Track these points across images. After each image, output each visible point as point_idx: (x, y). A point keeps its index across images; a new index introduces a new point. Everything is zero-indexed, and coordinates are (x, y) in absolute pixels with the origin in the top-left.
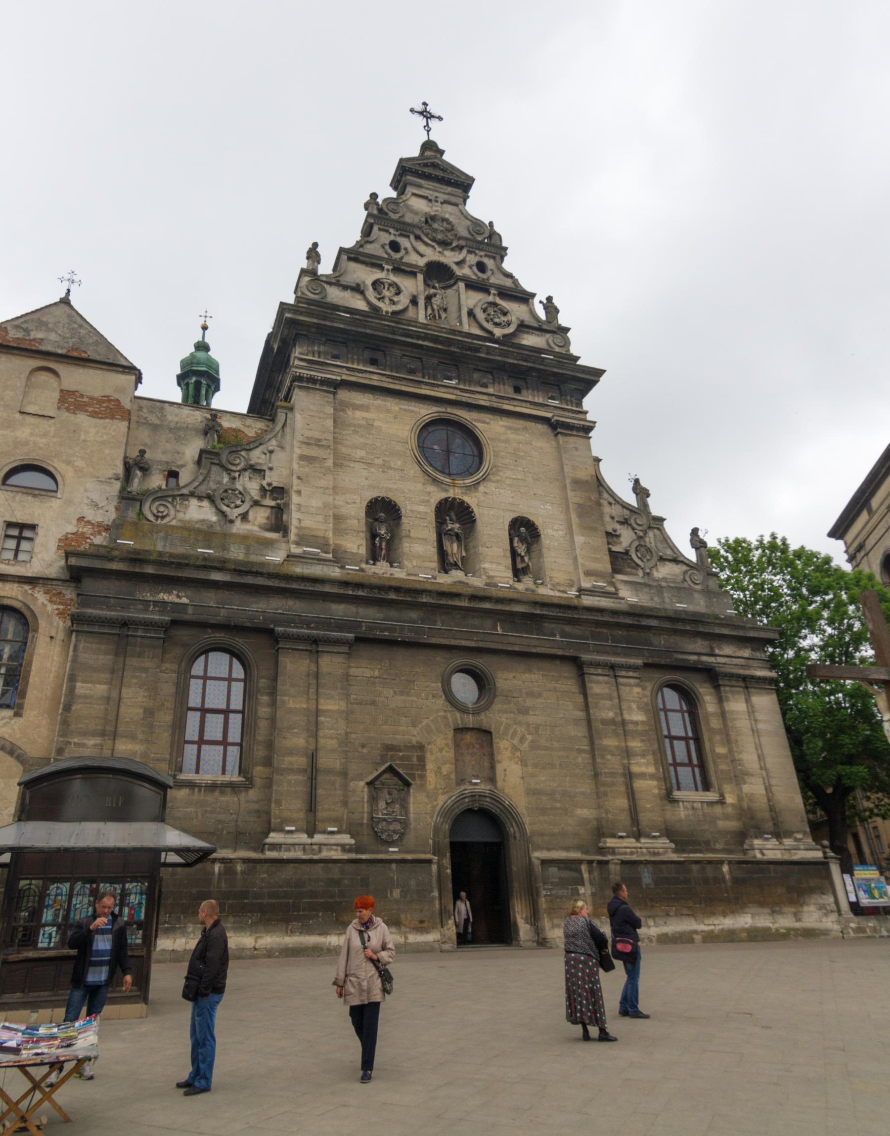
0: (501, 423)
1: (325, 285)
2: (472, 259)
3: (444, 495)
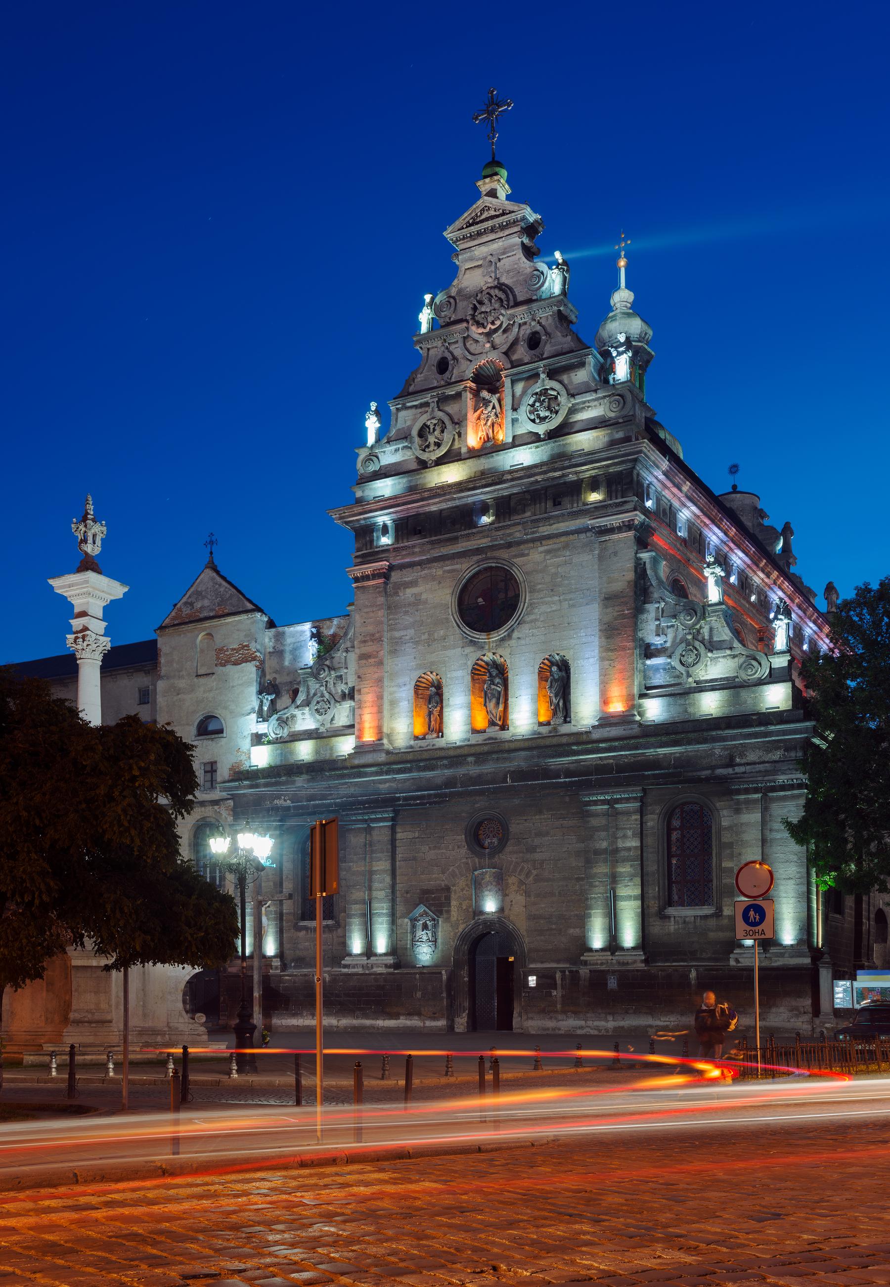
0: (541, 549)
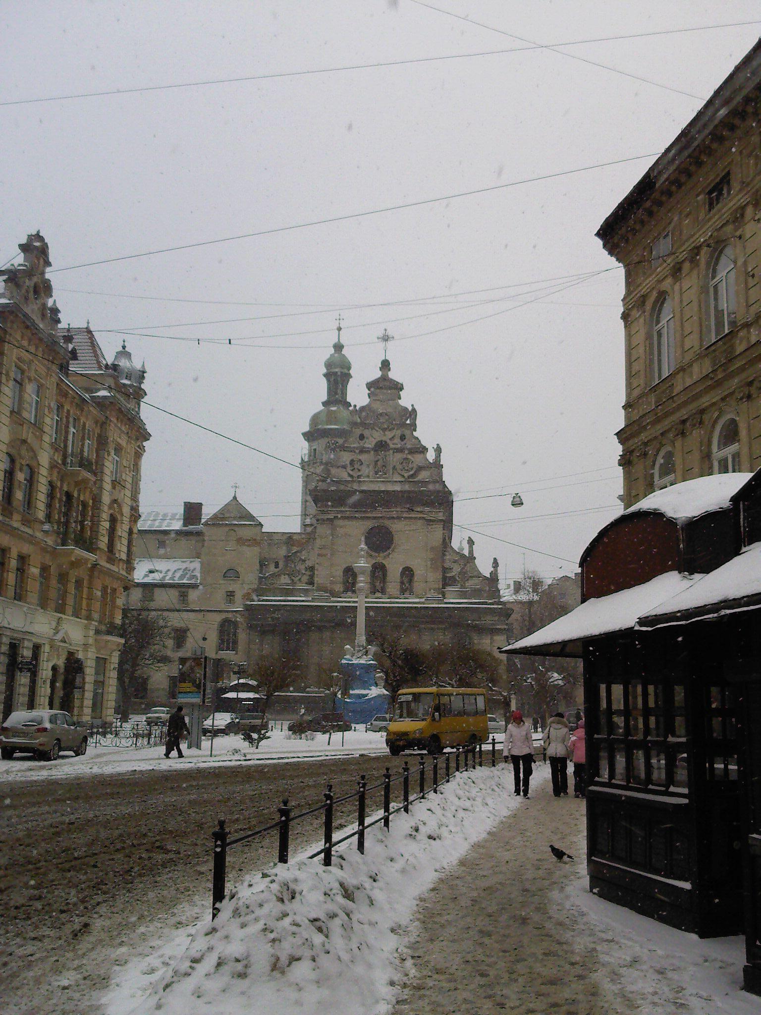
1: (330, 468)
2: (398, 433)
3: (374, 561)
